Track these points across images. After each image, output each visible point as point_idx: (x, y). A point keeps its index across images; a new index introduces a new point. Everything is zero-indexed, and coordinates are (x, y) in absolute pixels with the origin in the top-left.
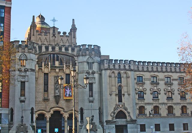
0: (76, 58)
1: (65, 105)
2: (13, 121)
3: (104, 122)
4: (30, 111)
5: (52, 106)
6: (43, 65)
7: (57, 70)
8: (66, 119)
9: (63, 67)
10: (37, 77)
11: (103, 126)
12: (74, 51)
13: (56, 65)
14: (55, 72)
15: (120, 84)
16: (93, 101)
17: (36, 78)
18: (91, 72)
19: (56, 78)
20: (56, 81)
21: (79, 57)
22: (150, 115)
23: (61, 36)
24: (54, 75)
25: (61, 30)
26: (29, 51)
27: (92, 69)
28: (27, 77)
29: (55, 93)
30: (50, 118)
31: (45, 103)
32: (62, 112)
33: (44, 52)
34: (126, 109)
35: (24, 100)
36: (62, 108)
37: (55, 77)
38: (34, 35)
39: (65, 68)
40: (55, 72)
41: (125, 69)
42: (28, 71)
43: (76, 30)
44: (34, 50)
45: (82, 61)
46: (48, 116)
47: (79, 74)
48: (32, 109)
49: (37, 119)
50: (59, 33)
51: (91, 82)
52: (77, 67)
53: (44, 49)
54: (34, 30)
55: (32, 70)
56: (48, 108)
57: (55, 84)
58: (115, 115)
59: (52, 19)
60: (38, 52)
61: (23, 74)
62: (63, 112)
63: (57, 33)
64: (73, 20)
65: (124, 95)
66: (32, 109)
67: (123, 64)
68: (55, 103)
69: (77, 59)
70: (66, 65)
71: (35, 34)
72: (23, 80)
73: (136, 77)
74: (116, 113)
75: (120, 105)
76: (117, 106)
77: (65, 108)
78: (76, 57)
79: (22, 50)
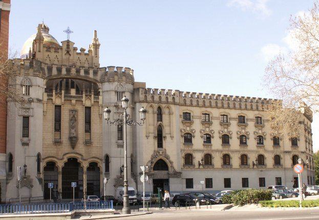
0: (99, 85)
1: (83, 150)
4: (36, 158)
5: (66, 152)
7: (74, 101)
8: (85, 170)
9: (82, 97)
10: (45, 110)
12: (97, 76)
13: (71, 95)
15: (160, 122)
17: (44, 112)
20: (72, 116)
22: (199, 166)
23: (78, 54)
24: (68, 108)
25: (78, 45)
28: (31, 110)
29: (70, 133)
32: (80, 160)
33: (55, 76)
34: (168, 158)
36: (81, 155)
38: (39, 51)
39: (84, 99)
40: (71, 104)
41: (167, 102)
44: (41, 72)
46: (60, 164)
48: (39, 155)
49: (45, 169)
50: (75, 49)
53: (55, 72)
54: (40, 44)
55: (39, 101)
56: (60, 154)
57: (71, 120)
58: (153, 165)
59: (66, 29)
60: (47, 75)
61: (26, 106)
63: (71, 49)
65: (165, 137)
66: (39, 155)
67: (165, 96)
68: (70, 147)
70: (87, 94)
71: (41, 50)
73: (182, 114)
74: (155, 162)
76: (156, 154)
77: (84, 155)
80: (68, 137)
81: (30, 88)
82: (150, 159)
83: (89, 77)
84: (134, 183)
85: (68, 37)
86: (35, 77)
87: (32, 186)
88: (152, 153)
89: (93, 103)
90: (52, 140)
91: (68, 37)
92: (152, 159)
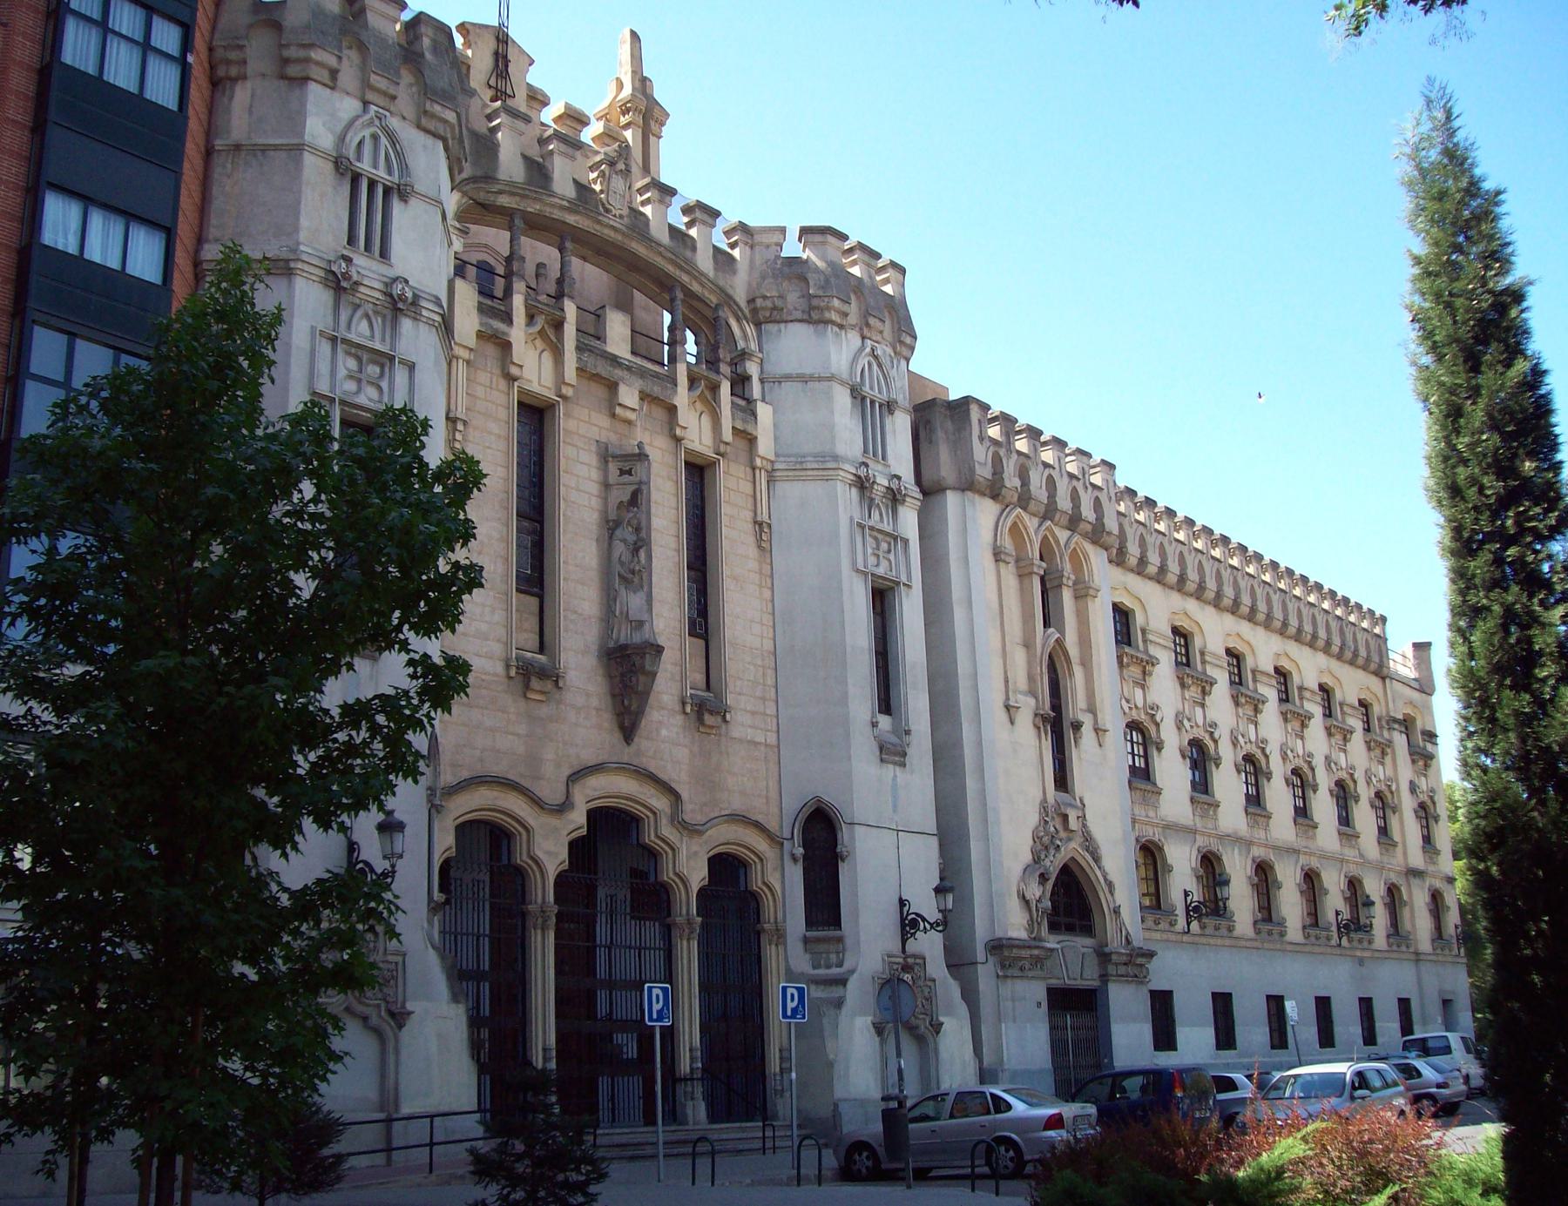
0: (743, 333)
1: (682, 754)
3: (980, 955)
5: (589, 757)
6: (518, 301)
10: (460, 413)
11: (970, 996)
12: (734, 272)
14: (612, 404)
16: (904, 754)
18: (883, 481)
19: (622, 472)
21: (772, 328)
24: (594, 433)
26: (437, 108)
27: (884, 458)
30: (561, 879)
31: (522, 703)
33: (512, 189)
37: (605, 455)
40: (612, 404)
43: (662, 124)
45: (807, 370)
47: (782, 488)
50: (538, 99)
51: (881, 571)
52: (764, 411)
56: (548, 769)
58: (1049, 885)
61: (360, 331)
62: (667, 831)
64: (634, 36)
65: (1077, 726)
68: (607, 720)
69: (753, 346)
72: (362, 400)
75: (1065, 817)
77: (685, 795)
78: (750, 330)
79: (374, 79)
80: (594, 648)
81: (397, 206)
82: (1027, 857)
84: (963, 1010)
86: (430, 141)
87: (399, 1017)
88: (1033, 819)
89: (727, 435)
90: (497, 649)
92: (1037, 860)
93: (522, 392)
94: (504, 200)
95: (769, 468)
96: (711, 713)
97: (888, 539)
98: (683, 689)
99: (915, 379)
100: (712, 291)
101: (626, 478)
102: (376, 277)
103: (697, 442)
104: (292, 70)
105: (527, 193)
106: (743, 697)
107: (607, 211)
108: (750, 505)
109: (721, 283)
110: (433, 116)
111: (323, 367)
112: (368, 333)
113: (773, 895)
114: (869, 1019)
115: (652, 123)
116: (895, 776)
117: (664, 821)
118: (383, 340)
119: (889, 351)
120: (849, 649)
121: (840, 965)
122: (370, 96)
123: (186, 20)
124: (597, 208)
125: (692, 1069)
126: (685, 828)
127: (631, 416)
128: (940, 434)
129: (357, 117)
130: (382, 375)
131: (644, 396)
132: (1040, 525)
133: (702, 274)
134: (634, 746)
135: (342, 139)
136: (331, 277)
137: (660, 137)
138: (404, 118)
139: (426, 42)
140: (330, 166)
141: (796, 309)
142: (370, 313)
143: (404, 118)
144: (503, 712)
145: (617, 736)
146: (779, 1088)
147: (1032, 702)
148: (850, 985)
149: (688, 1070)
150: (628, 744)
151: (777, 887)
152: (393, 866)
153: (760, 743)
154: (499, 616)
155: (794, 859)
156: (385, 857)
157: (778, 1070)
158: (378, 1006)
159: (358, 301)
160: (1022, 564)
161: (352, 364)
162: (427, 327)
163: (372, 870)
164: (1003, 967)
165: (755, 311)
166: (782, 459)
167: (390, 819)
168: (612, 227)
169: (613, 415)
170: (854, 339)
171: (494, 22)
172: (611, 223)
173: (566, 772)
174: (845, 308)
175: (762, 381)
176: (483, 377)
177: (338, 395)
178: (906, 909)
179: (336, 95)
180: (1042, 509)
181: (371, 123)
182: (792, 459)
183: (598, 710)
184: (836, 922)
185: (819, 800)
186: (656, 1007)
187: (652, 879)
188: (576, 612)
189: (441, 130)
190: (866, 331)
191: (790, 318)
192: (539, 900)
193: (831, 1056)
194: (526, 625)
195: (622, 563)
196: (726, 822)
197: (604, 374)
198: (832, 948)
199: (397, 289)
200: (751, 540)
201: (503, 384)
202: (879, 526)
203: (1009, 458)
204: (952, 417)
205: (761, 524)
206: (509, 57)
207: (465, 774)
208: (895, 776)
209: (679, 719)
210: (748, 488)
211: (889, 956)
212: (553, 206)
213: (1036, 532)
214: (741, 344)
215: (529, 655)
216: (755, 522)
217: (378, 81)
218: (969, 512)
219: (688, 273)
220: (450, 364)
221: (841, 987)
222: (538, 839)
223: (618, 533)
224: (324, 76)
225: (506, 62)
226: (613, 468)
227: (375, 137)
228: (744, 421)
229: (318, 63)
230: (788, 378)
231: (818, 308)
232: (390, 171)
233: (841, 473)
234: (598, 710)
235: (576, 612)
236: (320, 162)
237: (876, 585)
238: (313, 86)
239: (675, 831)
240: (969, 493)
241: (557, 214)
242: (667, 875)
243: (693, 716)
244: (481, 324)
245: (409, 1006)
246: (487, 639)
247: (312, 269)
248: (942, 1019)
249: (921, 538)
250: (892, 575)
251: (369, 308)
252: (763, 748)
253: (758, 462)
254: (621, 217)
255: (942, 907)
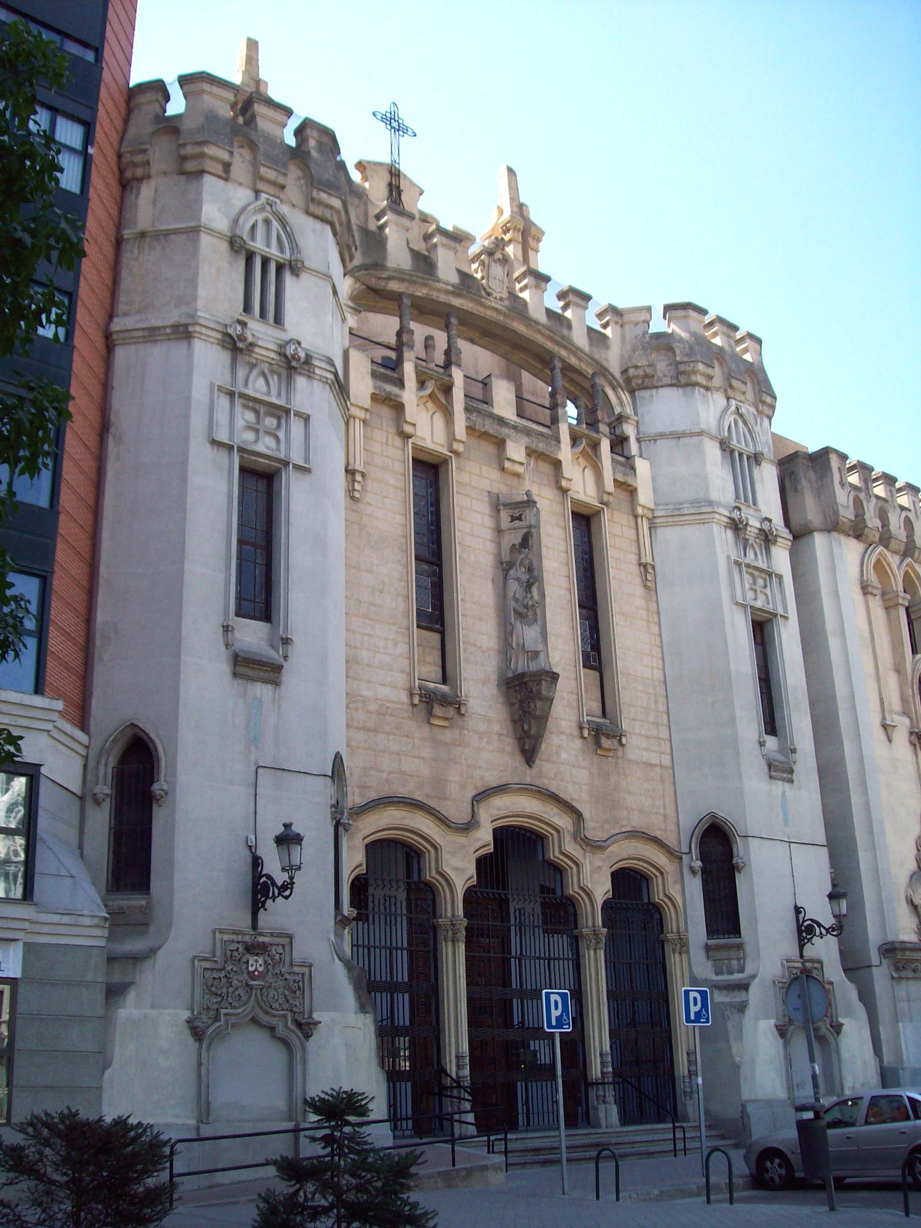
0: (620, 401)
1: (582, 775)
2: (154, 884)
3: (875, 958)
5: (493, 778)
6: (409, 369)
10: (359, 466)
11: (867, 998)
12: (607, 347)
16: (791, 771)
18: (755, 523)
19: (513, 519)
24: (486, 485)
26: (323, 196)
27: (755, 503)
31: (426, 729)
33: (399, 274)
35: (274, 655)
37: (497, 504)
42: (310, 376)
45: (679, 428)
47: (661, 532)
51: (759, 604)
52: (642, 466)
56: (453, 789)
59: (384, 108)
61: (257, 387)
62: (571, 848)
64: (510, 171)
68: (509, 744)
72: (260, 448)
77: (586, 814)
78: (626, 397)
79: (263, 171)
80: (494, 678)
81: (289, 280)
83: (570, 342)
84: (860, 1010)
85: (394, 148)
86: (318, 225)
87: (306, 1028)
89: (609, 486)
90: (401, 680)
91: (394, 148)
93: (416, 448)
94: (394, 286)
95: (650, 516)
96: (608, 736)
97: (763, 575)
98: (580, 714)
99: (778, 440)
100: (588, 364)
101: (517, 523)
102: (270, 339)
103: (582, 492)
104: (190, 166)
105: (414, 278)
106: (637, 723)
107: (489, 294)
108: (635, 550)
109: (597, 356)
110: (320, 203)
111: (222, 417)
112: (265, 389)
113: (675, 907)
114: (772, 1022)
115: (530, 240)
116: (784, 793)
117: (567, 838)
118: (279, 395)
119: (752, 410)
120: (733, 676)
121: (742, 970)
122: (261, 186)
123: (88, 119)
124: (479, 290)
125: (602, 1073)
126: (588, 844)
127: (520, 469)
128: (804, 483)
129: (249, 204)
130: (279, 426)
131: (531, 452)
132: (902, 562)
133: (578, 348)
134: (535, 770)
135: (236, 221)
136: (228, 339)
137: (537, 251)
138: (294, 206)
139: (312, 143)
140: (224, 246)
141: (665, 376)
142: (266, 371)
143: (294, 206)
144: (408, 737)
145: (519, 759)
146: (688, 1090)
147: (907, 721)
148: (753, 989)
149: (599, 1075)
150: (530, 767)
151: (679, 899)
152: (291, 878)
153: (655, 765)
154: (402, 649)
155: (693, 872)
156: (283, 869)
157: (686, 1072)
158: (285, 1016)
159: (254, 361)
160: (887, 597)
161: (250, 416)
162: (321, 384)
163: (274, 883)
164: (897, 969)
165: (628, 380)
166: (661, 507)
167: (288, 832)
168: (495, 309)
169: (503, 469)
170: (719, 400)
171: (388, 161)
172: (493, 304)
173: (473, 793)
174: (710, 371)
175: (639, 440)
176: (379, 435)
177: (236, 442)
178: (802, 915)
179: (230, 186)
180: (902, 548)
181: (262, 209)
182: (671, 507)
183: (500, 735)
184: (735, 929)
185: (713, 816)
186: (555, 1013)
187: (559, 893)
188: (475, 645)
189: (328, 214)
190: (730, 392)
191: (660, 384)
192: (449, 914)
193: (737, 1059)
194: (429, 659)
195: (516, 600)
196: (626, 838)
197: (491, 432)
198: (733, 954)
199: (291, 350)
200: (637, 581)
201: (398, 441)
202: (755, 564)
203: (869, 501)
204: (813, 467)
205: (645, 566)
206: (402, 187)
207: (374, 795)
208: (784, 793)
209: (578, 743)
210: (631, 534)
211: (788, 961)
212: (439, 290)
213: (899, 567)
214: (618, 410)
215: (432, 685)
216: (640, 564)
217: (271, 174)
218: (836, 551)
219: (565, 348)
220: (347, 423)
221: (743, 993)
222: (446, 855)
223: (512, 573)
224: (218, 169)
225: (399, 193)
226: (505, 515)
227: (267, 222)
228: (625, 474)
229: (212, 158)
230: (662, 436)
231: (684, 373)
232: (282, 250)
233: (717, 516)
234: (500, 735)
235: (475, 645)
236: (215, 241)
237: (757, 618)
238: (208, 180)
239: (578, 847)
240: (835, 534)
241: (443, 298)
242: (572, 889)
243: (591, 740)
244: (375, 388)
245: (316, 1016)
246: (391, 670)
247: (209, 333)
248: (841, 1020)
249: (795, 577)
250: (770, 608)
251: (265, 368)
252: (658, 769)
253: (640, 511)
254: (501, 299)
255: (837, 913)
